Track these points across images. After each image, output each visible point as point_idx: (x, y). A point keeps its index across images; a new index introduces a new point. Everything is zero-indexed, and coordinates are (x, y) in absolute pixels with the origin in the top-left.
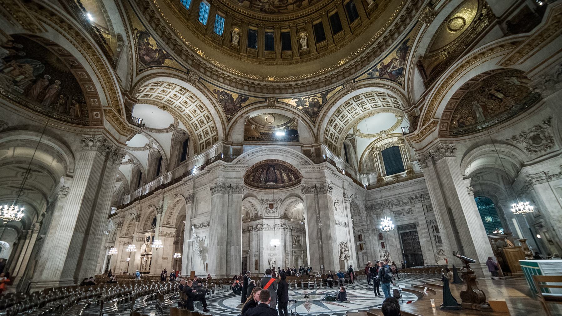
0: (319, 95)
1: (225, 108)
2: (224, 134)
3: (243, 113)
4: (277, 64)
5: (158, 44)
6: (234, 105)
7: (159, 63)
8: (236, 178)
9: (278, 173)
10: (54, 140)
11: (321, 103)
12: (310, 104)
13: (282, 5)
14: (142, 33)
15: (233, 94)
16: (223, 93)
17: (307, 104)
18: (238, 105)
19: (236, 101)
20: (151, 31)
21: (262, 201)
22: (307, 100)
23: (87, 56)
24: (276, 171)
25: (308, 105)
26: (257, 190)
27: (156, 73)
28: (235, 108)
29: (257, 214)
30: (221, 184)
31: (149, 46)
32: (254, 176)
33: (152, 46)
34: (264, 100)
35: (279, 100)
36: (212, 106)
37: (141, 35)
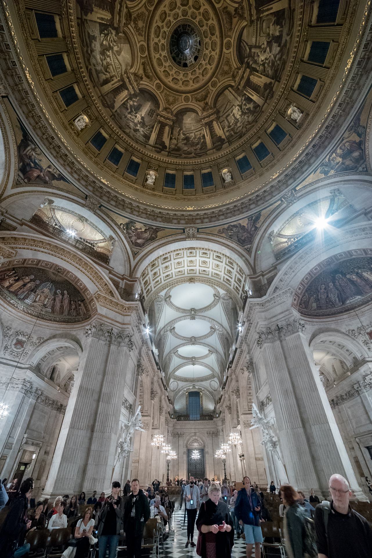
2: (248, 268)
3: (263, 233)
4: (278, 161)
5: (145, 225)
6: (248, 232)
8: (282, 313)
9: (354, 277)
10: (68, 340)
11: (358, 139)
13: (257, 114)
17: (340, 159)
18: (253, 229)
20: (135, 218)
21: (351, 334)
23: (66, 259)
24: (348, 276)
25: (340, 160)
26: (334, 319)
28: (251, 234)
29: (355, 358)
30: (264, 330)
32: (317, 300)
35: (297, 188)
36: (223, 247)
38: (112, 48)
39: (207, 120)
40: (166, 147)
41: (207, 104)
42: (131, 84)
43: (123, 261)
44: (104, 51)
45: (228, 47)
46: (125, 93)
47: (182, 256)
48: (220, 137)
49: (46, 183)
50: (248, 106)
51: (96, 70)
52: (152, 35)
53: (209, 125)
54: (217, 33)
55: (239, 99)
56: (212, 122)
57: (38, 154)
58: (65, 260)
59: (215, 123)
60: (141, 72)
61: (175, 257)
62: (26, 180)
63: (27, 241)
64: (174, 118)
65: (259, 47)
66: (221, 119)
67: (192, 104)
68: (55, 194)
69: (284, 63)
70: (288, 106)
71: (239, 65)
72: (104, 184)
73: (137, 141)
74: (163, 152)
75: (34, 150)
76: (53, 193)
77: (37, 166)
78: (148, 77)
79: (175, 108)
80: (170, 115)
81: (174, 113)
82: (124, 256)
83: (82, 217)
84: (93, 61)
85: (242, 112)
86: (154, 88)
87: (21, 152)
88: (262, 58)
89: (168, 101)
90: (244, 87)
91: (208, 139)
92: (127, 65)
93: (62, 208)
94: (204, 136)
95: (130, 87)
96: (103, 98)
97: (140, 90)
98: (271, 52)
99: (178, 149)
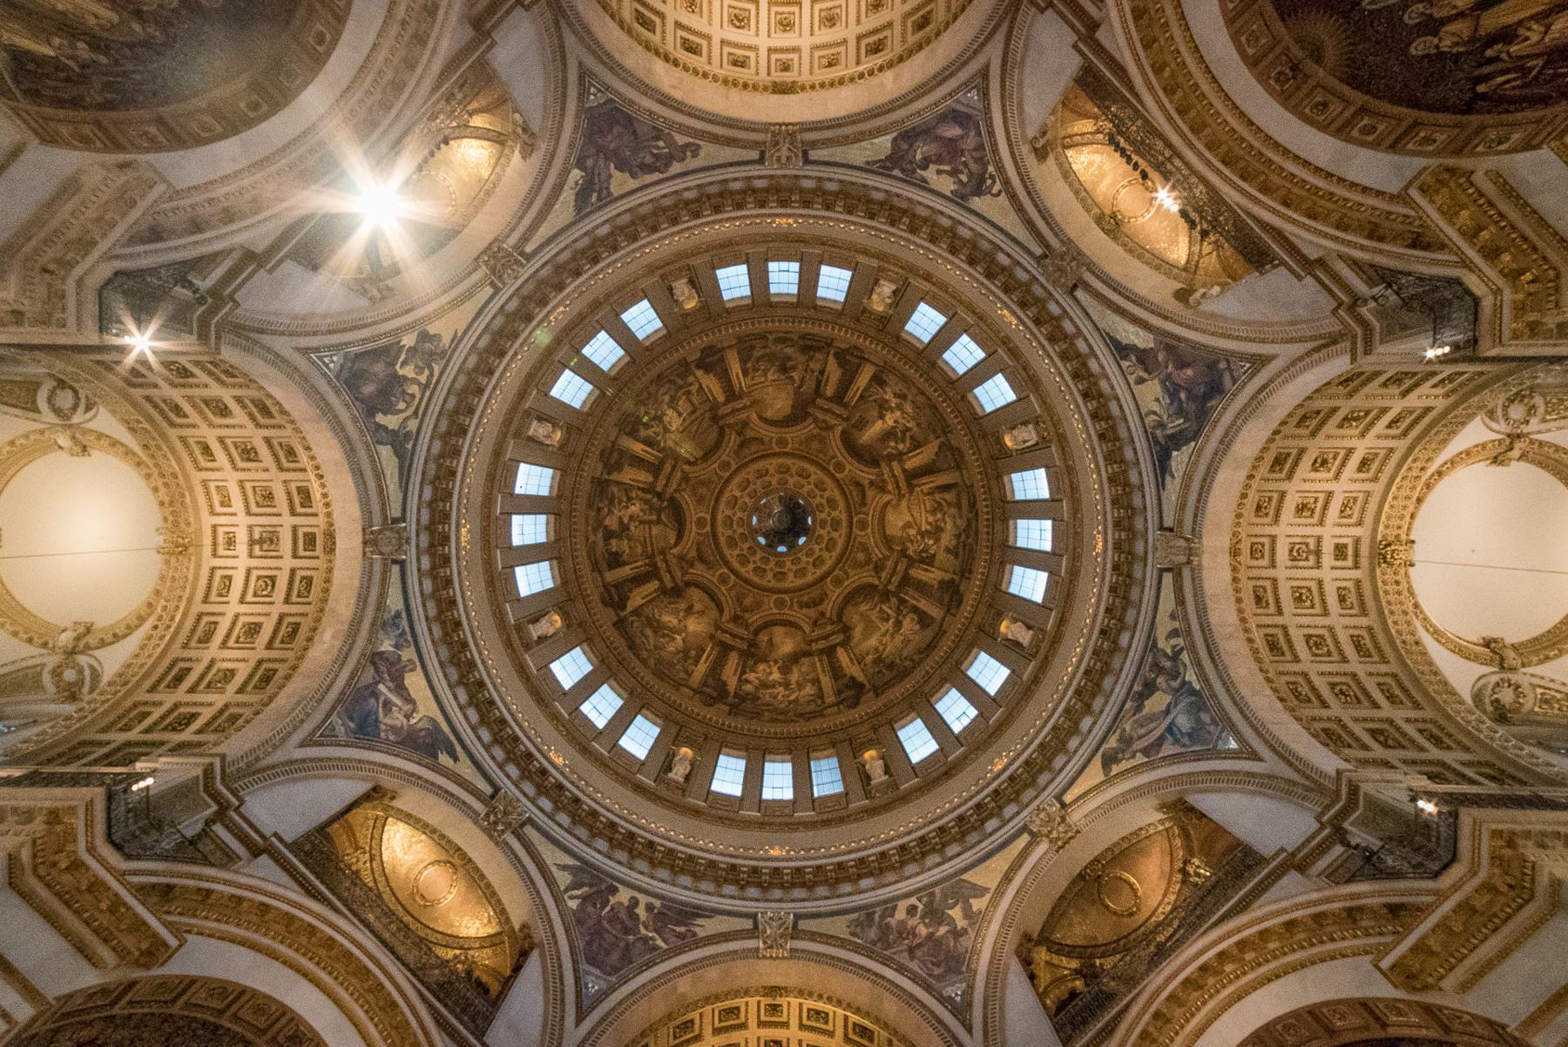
0: (413, 425)
1: (629, 120)
5: (923, 185)
7: (909, 136)
12: (398, 380)
14: (978, 192)
15: (633, 184)
16: (661, 163)
19: (607, 167)
22: (423, 379)
27: (912, 101)
31: (947, 168)
33: (939, 172)
34: (529, 248)
36: (677, 95)
37: (982, 181)
38: (919, 532)
39: (739, 404)
40: (836, 355)
41: (739, 434)
42: (894, 476)
43: (1028, 62)
44: (937, 531)
45: (701, 523)
46: (909, 465)
47: (817, 54)
48: (707, 371)
49: (1171, 345)
50: (650, 432)
51: (959, 506)
52: (841, 543)
53: (732, 395)
54: (722, 541)
55: (670, 443)
56: (728, 401)
57: (1155, 413)
58: (1242, 115)
59: (721, 398)
60: (870, 493)
61: (842, 49)
62: (1222, 365)
63: (1336, 216)
64: (811, 410)
65: (641, 522)
66: (707, 406)
67: (770, 433)
68: (1160, 315)
69: (590, 505)
70: (562, 447)
71: (677, 495)
72: (1014, 313)
73: (904, 378)
74: (844, 346)
75: (1161, 425)
76: (1166, 318)
77: (1172, 390)
78: (857, 484)
79: (808, 428)
80: (820, 416)
81: (810, 420)
82: (1021, 85)
83: (1107, 232)
84: (961, 523)
85: (661, 421)
86: (848, 467)
87: (1195, 428)
88: (635, 509)
89: (822, 441)
90: (662, 462)
91: (735, 368)
92: (898, 505)
93: (1158, 268)
94: (745, 373)
95: (898, 472)
96: (959, 464)
97: (878, 466)
98: (621, 519)
99: (805, 349)
